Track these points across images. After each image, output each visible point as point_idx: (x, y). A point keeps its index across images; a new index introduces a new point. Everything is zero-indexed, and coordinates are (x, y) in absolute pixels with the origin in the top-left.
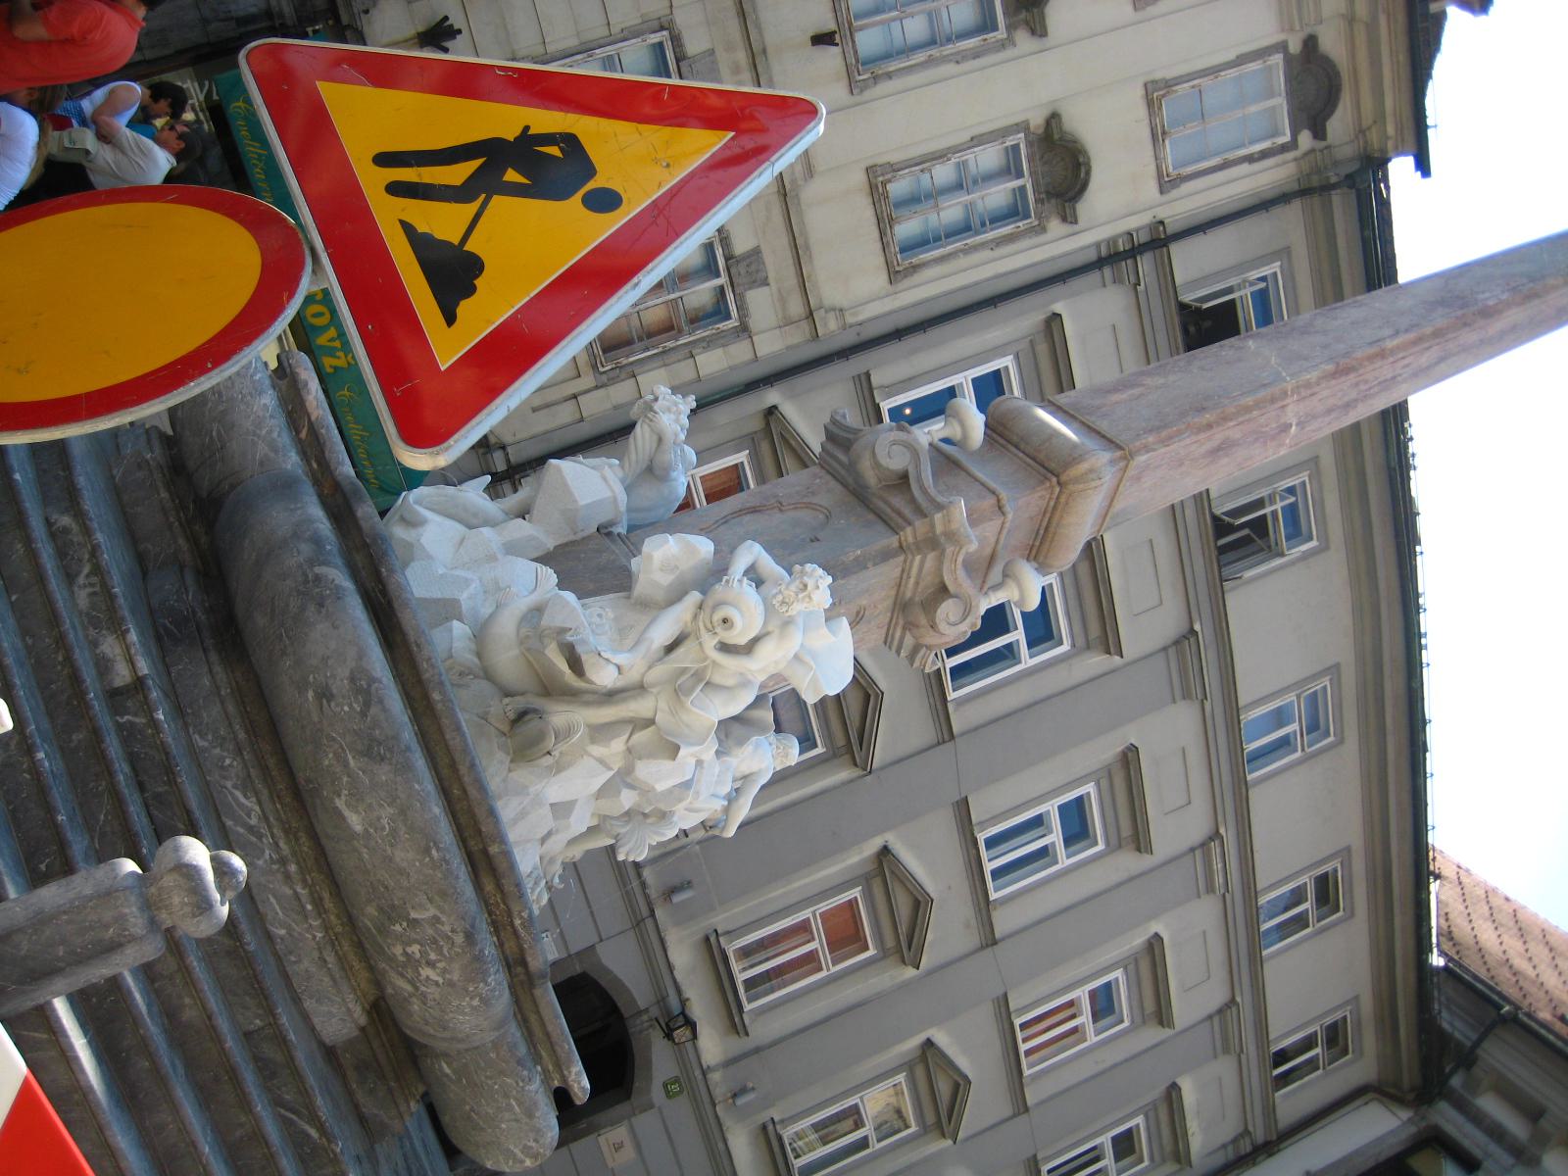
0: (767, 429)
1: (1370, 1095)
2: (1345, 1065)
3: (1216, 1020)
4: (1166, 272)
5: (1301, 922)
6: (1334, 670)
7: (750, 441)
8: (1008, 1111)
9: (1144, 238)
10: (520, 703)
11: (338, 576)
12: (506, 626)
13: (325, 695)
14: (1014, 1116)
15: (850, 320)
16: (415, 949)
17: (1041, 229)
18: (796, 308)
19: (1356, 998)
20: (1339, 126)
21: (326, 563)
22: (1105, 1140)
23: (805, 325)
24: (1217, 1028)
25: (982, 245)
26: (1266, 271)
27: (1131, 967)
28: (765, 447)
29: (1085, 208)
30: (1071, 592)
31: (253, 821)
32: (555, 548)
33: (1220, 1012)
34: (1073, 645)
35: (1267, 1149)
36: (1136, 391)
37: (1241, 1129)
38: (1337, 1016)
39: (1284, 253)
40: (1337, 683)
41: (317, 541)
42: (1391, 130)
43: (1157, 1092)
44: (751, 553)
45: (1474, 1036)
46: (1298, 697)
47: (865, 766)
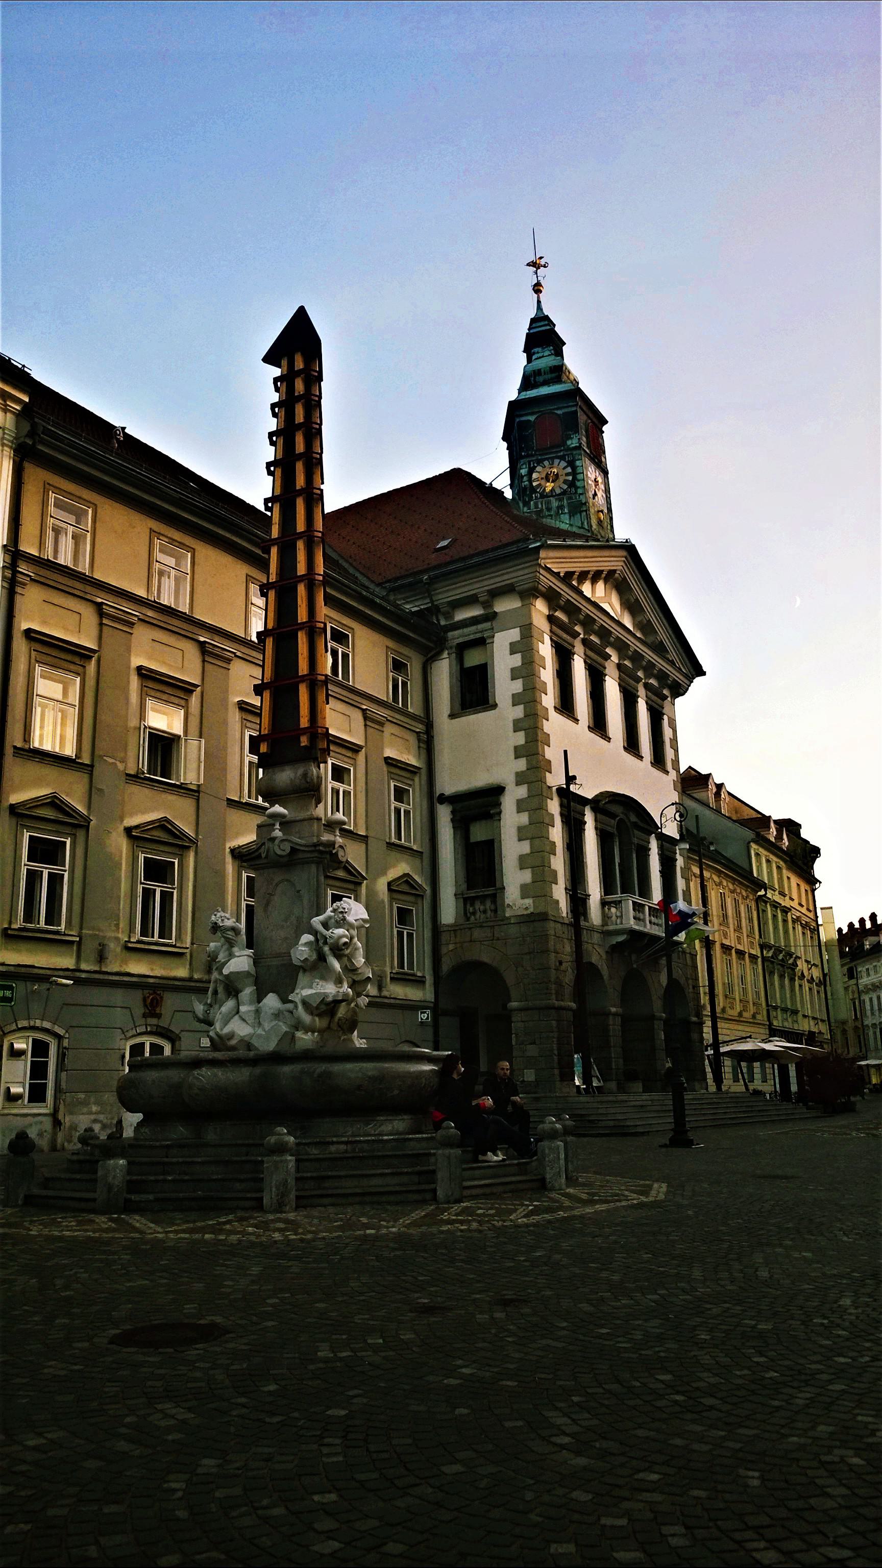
8: (364, 846)
9: (8, 560)
14: (367, 844)
19: (387, 647)
22: (394, 804)
24: (373, 725)
35: (429, 725)
38: (390, 660)
43: (385, 768)
44: (316, 921)
45: (428, 600)
47: (194, 842)
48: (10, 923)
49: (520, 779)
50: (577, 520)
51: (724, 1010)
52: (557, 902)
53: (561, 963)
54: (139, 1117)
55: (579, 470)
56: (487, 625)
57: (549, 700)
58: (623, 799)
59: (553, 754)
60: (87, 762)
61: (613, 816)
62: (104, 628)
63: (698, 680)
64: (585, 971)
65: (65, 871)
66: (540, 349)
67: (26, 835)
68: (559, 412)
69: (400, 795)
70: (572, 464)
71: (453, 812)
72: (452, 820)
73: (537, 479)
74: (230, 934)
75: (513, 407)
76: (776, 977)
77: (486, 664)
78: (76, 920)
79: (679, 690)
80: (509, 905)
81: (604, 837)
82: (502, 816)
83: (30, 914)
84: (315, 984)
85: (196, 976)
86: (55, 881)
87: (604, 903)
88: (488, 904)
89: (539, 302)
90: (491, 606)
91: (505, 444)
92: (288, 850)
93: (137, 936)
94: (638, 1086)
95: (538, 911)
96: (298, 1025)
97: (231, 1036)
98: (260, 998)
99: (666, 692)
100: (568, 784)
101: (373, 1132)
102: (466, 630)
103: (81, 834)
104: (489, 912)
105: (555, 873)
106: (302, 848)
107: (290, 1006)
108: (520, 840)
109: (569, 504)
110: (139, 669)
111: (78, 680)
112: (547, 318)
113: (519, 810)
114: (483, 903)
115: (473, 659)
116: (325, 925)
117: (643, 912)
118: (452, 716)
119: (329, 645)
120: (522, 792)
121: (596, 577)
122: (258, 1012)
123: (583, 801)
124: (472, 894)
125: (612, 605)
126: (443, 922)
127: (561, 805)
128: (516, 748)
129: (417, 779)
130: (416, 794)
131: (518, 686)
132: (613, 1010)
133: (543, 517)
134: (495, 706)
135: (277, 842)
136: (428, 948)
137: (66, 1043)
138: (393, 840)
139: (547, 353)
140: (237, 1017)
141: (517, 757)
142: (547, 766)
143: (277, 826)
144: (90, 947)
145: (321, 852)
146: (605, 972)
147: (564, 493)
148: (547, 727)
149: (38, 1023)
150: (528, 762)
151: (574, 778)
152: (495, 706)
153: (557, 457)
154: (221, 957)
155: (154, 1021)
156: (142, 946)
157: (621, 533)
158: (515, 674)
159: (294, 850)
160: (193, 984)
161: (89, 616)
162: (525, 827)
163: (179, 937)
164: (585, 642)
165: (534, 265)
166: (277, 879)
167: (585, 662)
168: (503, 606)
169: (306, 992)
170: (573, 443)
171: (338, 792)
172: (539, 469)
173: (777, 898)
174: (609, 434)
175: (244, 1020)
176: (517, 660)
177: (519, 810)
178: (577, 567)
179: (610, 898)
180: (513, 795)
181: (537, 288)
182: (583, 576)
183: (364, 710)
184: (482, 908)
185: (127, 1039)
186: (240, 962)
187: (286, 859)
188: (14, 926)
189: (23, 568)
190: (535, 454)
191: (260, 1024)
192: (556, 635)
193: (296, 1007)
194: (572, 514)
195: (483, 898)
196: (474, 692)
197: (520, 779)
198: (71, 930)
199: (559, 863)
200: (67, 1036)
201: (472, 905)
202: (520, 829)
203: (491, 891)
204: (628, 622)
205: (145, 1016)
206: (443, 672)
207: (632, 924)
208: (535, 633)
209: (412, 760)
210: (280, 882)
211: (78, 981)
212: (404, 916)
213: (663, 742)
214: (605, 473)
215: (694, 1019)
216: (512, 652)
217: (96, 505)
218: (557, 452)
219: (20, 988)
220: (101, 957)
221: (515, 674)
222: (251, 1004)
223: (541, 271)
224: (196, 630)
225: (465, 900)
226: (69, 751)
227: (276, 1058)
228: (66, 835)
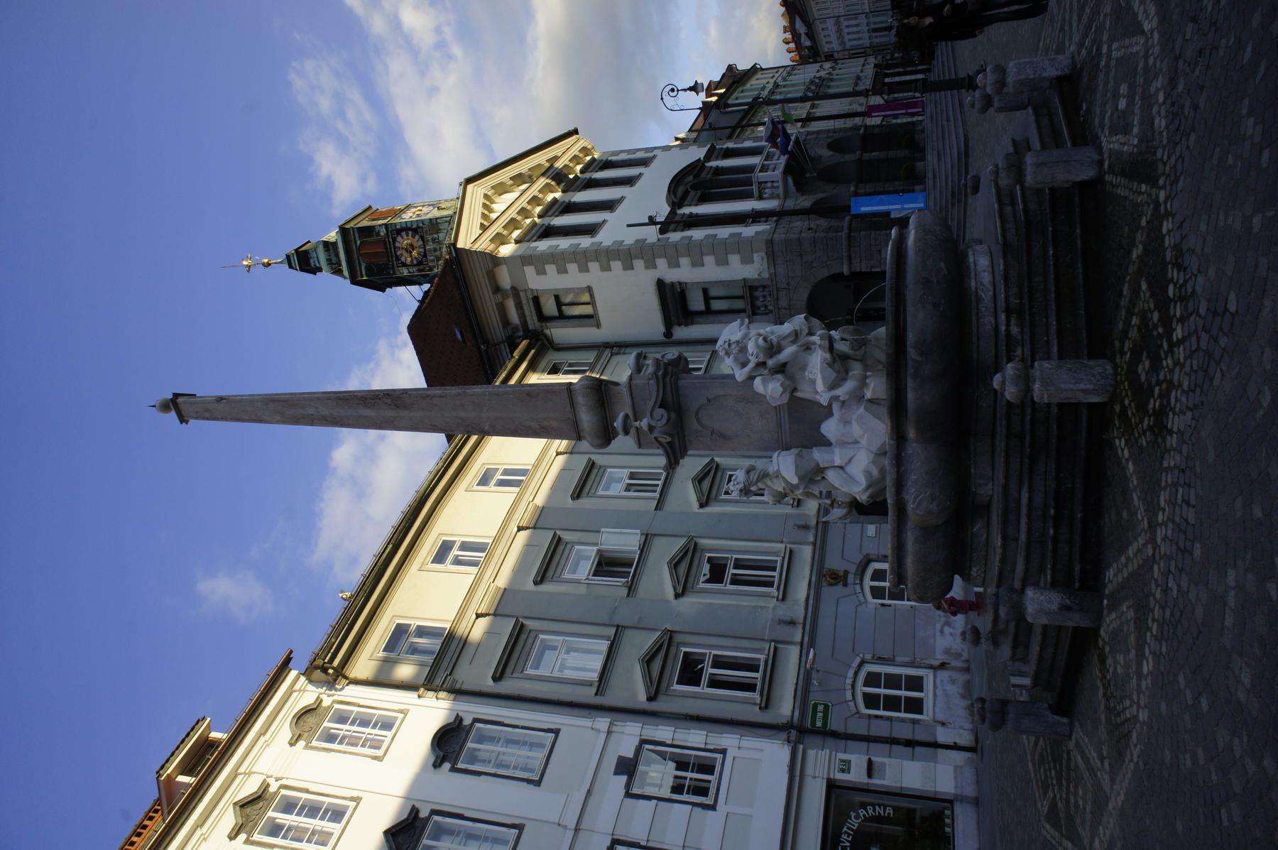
11: (912, 353)
17: (476, 720)
35: (607, 346)
36: (545, 423)
47: (691, 539)
54: (957, 577)
56: (522, 294)
57: (585, 242)
59: (630, 236)
60: (613, 630)
61: (686, 194)
62: (499, 612)
64: (817, 210)
67: (676, 687)
70: (399, 232)
71: (679, 325)
72: (687, 325)
74: (754, 476)
75: (355, 282)
81: (703, 199)
83: (750, 687)
85: (811, 539)
86: (719, 663)
87: (761, 198)
88: (757, 294)
90: (506, 291)
92: (662, 411)
93: (773, 591)
94: (920, 165)
96: (858, 397)
97: (868, 473)
98: (828, 444)
99: (588, 158)
101: (991, 293)
102: (527, 313)
103: (678, 638)
105: (732, 235)
107: (835, 407)
110: (536, 583)
111: (542, 636)
112: (288, 257)
118: (598, 326)
120: (662, 263)
122: (843, 444)
123: (673, 213)
127: (675, 230)
128: (625, 269)
131: (572, 267)
134: (590, 289)
135: (653, 423)
137: (868, 657)
143: (637, 424)
144: (782, 632)
145: (665, 375)
147: (422, 238)
149: (849, 681)
150: (636, 258)
151: (651, 218)
154: (779, 486)
155: (851, 578)
158: (562, 270)
159: (663, 405)
163: (776, 554)
166: (695, 425)
168: (505, 281)
169: (820, 386)
170: (383, 232)
173: (766, 92)
175: (850, 460)
176: (551, 269)
179: (756, 193)
182: (484, 216)
185: (866, 602)
186: (785, 466)
187: (673, 415)
188: (758, 701)
193: (836, 398)
194: (438, 231)
197: (651, 265)
199: (723, 232)
201: (758, 308)
202: (694, 264)
205: (845, 585)
206: (560, 333)
207: (778, 173)
208: (529, 253)
210: (698, 421)
211: (812, 644)
215: (862, 131)
219: (815, 697)
220: (792, 623)
221: (562, 270)
224: (507, 533)
226: (604, 646)
227: (897, 410)
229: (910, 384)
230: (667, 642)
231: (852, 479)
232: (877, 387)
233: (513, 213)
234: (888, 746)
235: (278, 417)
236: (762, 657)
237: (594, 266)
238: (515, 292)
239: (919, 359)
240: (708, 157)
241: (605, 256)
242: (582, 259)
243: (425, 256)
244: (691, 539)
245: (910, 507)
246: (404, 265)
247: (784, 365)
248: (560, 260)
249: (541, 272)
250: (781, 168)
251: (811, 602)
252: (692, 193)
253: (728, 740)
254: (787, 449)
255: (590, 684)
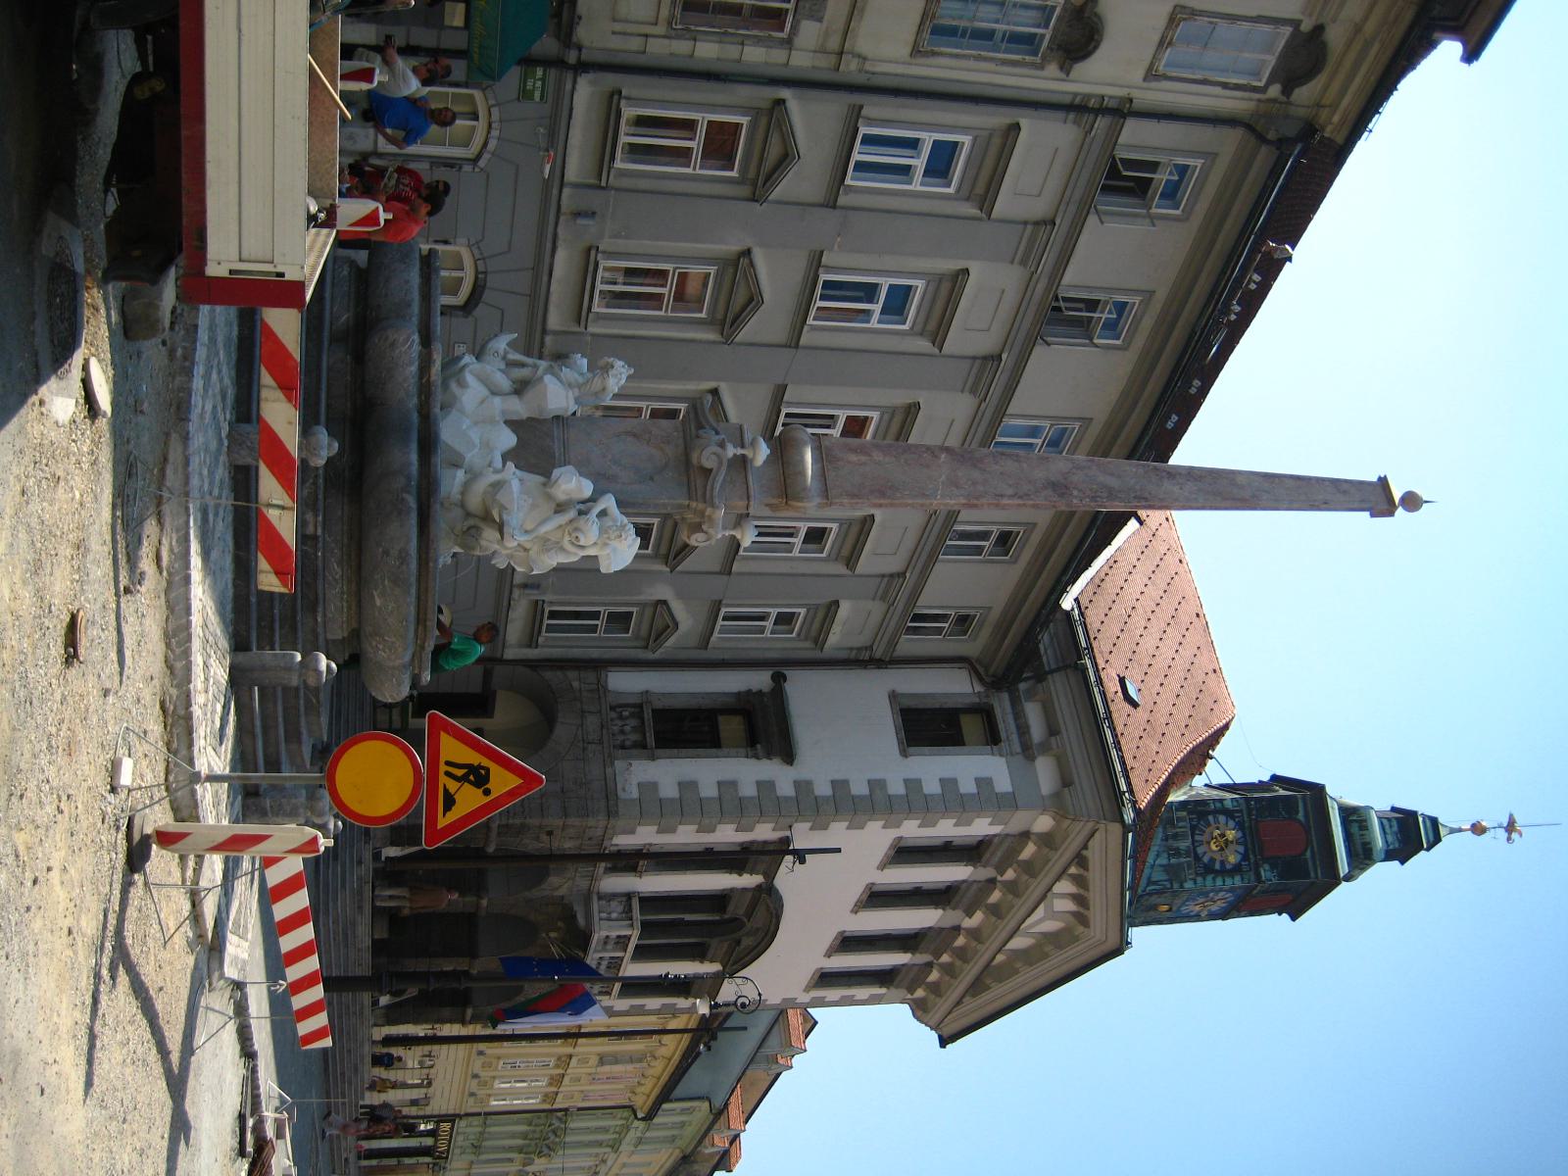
0: (771, 112)
1: (966, 665)
2: (962, 640)
3: (886, 579)
4: (1114, 134)
5: (979, 550)
6: (1086, 421)
7: (755, 112)
8: (717, 568)
9: (1112, 104)
10: (471, 522)
11: (412, 502)
12: (481, 486)
13: (386, 553)
15: (868, 67)
16: (381, 647)
17: (1041, 67)
18: (834, 43)
19: (990, 608)
20: (1303, 94)
21: (408, 492)
22: (774, 612)
23: (833, 59)
24: (883, 585)
25: (991, 60)
26: (1191, 162)
27: (845, 526)
28: (764, 121)
29: (1081, 69)
30: (929, 296)
31: (337, 577)
32: (529, 419)
33: (892, 576)
34: (912, 328)
35: (879, 663)
36: (863, 458)
37: (868, 644)
38: (972, 612)
39: (1211, 156)
40: (1083, 430)
41: (409, 478)
42: (1336, 119)
44: (609, 502)
45: (1053, 666)
46: (1052, 425)
47: (728, 340)
48: (628, 98)
49: (803, 787)
50: (1159, 876)
51: (481, 1053)
52: (632, 832)
53: (550, 833)
55: (1229, 881)
56: (1017, 748)
57: (912, 830)
58: (772, 928)
59: (837, 833)
60: (842, 200)
61: (749, 914)
62: (1021, 227)
63: (934, 1036)
65: (694, 169)
66: (1395, 828)
67: (744, 120)
68: (1308, 854)
69: (785, 620)
70: (1237, 869)
72: (749, 692)
73: (1217, 821)
75: (1317, 791)
76: (524, 1128)
77: (964, 745)
78: (626, 183)
79: (920, 1010)
80: (631, 764)
82: (753, 761)
84: (525, 497)
85: (548, 339)
86: (682, 155)
89: (1460, 830)
91: (1266, 778)
92: (708, 465)
94: (382, 934)
95: (620, 805)
96: (473, 476)
97: (463, 385)
98: (510, 423)
99: (920, 993)
100: (795, 852)
103: (745, 191)
104: (621, 738)
106: (708, 488)
107: (498, 463)
108: (720, 784)
109: (1180, 865)
110: (967, 271)
112: (1437, 839)
113: (759, 784)
114: (634, 729)
115: (970, 726)
116: (603, 513)
117: (614, 950)
119: (994, 528)
120: (785, 789)
121: (1080, 900)
124: (648, 715)
125: (1042, 922)
126: (610, 674)
127: (765, 842)
129: (808, 644)
130: (787, 642)
131: (932, 787)
132: (484, 902)
133: (1165, 828)
134: (904, 754)
135: (719, 450)
136: (576, 653)
137: (467, 168)
138: (724, 610)
139: (1390, 838)
140: (485, 392)
141: (834, 783)
142: (820, 826)
146: (535, 893)
147: (1197, 858)
148: (874, 826)
149: (495, 133)
150: (826, 799)
151: (802, 861)
152: (904, 754)
153: (1246, 850)
156: (591, 268)
157: (1136, 934)
159: (707, 472)
160: (538, 336)
161: (1039, 208)
162: (736, 790)
163: (600, 317)
164: (992, 882)
165: (1511, 827)
167: (964, 881)
168: (1045, 771)
169: (515, 485)
170: (1265, 872)
171: (791, 535)
172: (1231, 823)
173: (632, 1135)
174: (1278, 922)
175: (482, 402)
176: (968, 786)
177: (759, 784)
178: (1094, 875)
180: (782, 777)
181: (1478, 829)
183: (904, 574)
184: (627, 728)
188: (623, 103)
189: (1102, 123)
190: (1251, 820)
191: (476, 423)
192: (1001, 843)
193: (496, 472)
194: (1167, 868)
195: (641, 729)
196: (926, 727)
197: (803, 787)
198: (615, 177)
199: (686, 836)
200: (477, 170)
201: (632, 715)
202: (733, 784)
203: (651, 740)
204: (1018, 943)
209: (836, 638)
211: (547, 184)
212: (620, 620)
213: (849, 985)
214: (1224, 915)
215: (469, 1012)
216: (978, 781)
217: (1187, 219)
218: (1254, 852)
222: (503, 412)
223: (1502, 834)
224: (1016, 350)
225: (638, 706)
227: (428, 443)
228: (744, 170)
229: (414, 469)
230: (759, 185)
231: (484, 381)
232: (452, 483)
233: (1036, 888)
234: (442, 46)
235: (1240, 480)
236: (618, 164)
237: (896, 788)
238: (1028, 751)
239: (405, 495)
240: (717, 980)
241: (874, 804)
242: (914, 801)
243: (1193, 828)
244: (728, 340)
245: (416, 337)
246: (1229, 814)
247: (556, 512)
248: (952, 801)
249: (984, 783)
250: (595, 938)
251: (549, 245)
252: (741, 912)
253: (664, 49)
254: (557, 417)
255: (872, 122)
